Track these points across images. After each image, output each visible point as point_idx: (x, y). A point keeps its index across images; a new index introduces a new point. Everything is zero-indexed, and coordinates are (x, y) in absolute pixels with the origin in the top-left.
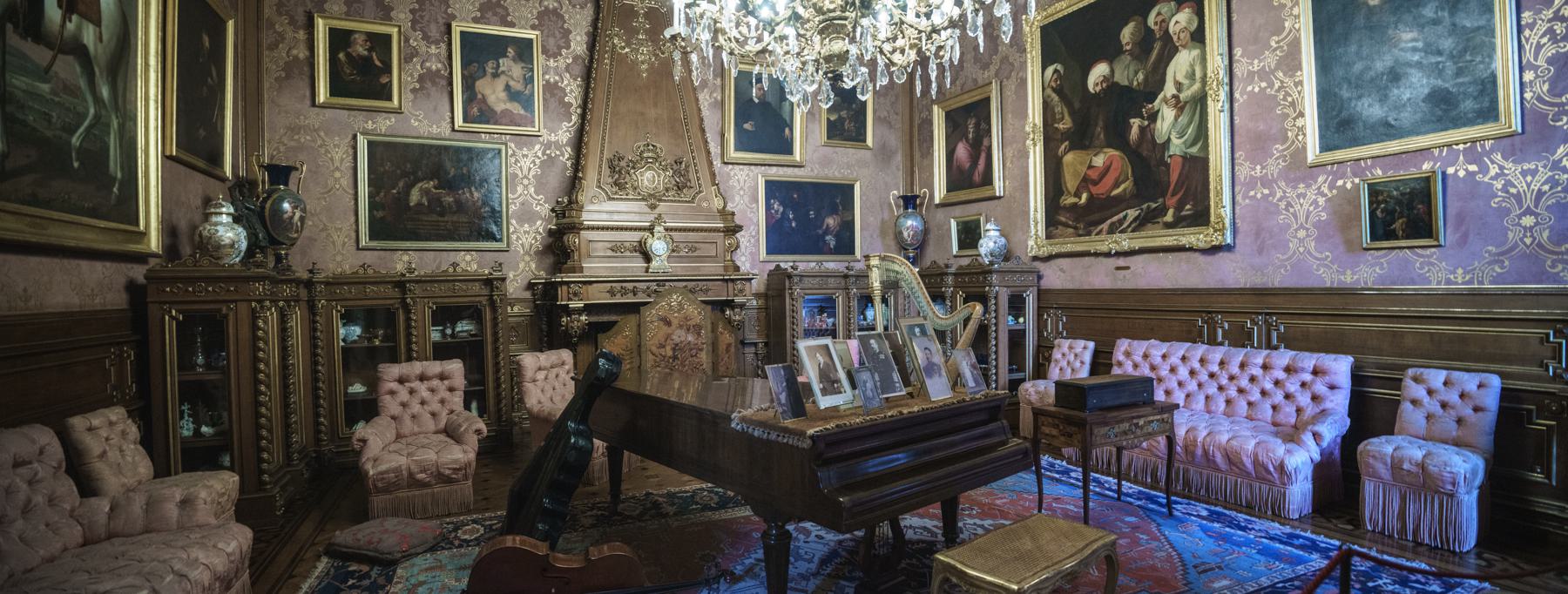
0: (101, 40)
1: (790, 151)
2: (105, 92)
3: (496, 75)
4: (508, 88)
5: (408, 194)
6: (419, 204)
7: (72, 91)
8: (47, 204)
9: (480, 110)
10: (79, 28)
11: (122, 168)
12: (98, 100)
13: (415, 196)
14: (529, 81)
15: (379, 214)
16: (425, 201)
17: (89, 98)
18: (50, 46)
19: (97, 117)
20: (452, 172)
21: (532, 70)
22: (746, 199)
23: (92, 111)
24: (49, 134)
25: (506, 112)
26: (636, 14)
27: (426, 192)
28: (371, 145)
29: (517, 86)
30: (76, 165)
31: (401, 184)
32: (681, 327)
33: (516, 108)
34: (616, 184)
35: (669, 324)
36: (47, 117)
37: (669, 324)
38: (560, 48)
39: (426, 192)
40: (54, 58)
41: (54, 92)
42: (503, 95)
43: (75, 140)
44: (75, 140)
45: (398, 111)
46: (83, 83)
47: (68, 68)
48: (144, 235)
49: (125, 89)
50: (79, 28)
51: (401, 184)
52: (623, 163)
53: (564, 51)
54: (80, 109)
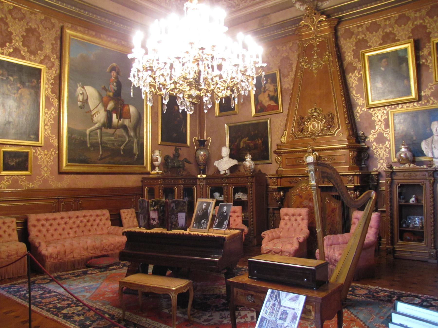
0: (131, 122)
1: (409, 93)
2: (132, 134)
3: (264, 92)
4: (269, 95)
5: (240, 144)
6: (243, 147)
7: (121, 136)
8: (114, 163)
9: (261, 107)
10: (123, 121)
11: (138, 151)
12: (129, 136)
13: (242, 144)
14: (276, 90)
15: (233, 152)
16: (245, 146)
17: (127, 137)
18: (114, 128)
19: (129, 141)
20: (252, 133)
21: (277, 86)
22: (383, 127)
23: (127, 139)
24: (114, 148)
25: (269, 106)
26: (314, 47)
27: (245, 142)
28: (230, 128)
29: (272, 94)
30: (122, 153)
31: (238, 140)
32: (306, 199)
33: (272, 103)
34: (299, 131)
35: (301, 197)
36: (114, 144)
37: (301, 197)
38: (289, 72)
39: (245, 142)
40: (115, 131)
41: (115, 138)
42: (267, 99)
43: (122, 148)
44: (122, 148)
45: (236, 114)
46: (124, 134)
47: (120, 132)
48: (145, 168)
49: (140, 131)
50: (123, 121)
51: (238, 140)
52: (303, 120)
53: (291, 73)
54: (124, 140)
